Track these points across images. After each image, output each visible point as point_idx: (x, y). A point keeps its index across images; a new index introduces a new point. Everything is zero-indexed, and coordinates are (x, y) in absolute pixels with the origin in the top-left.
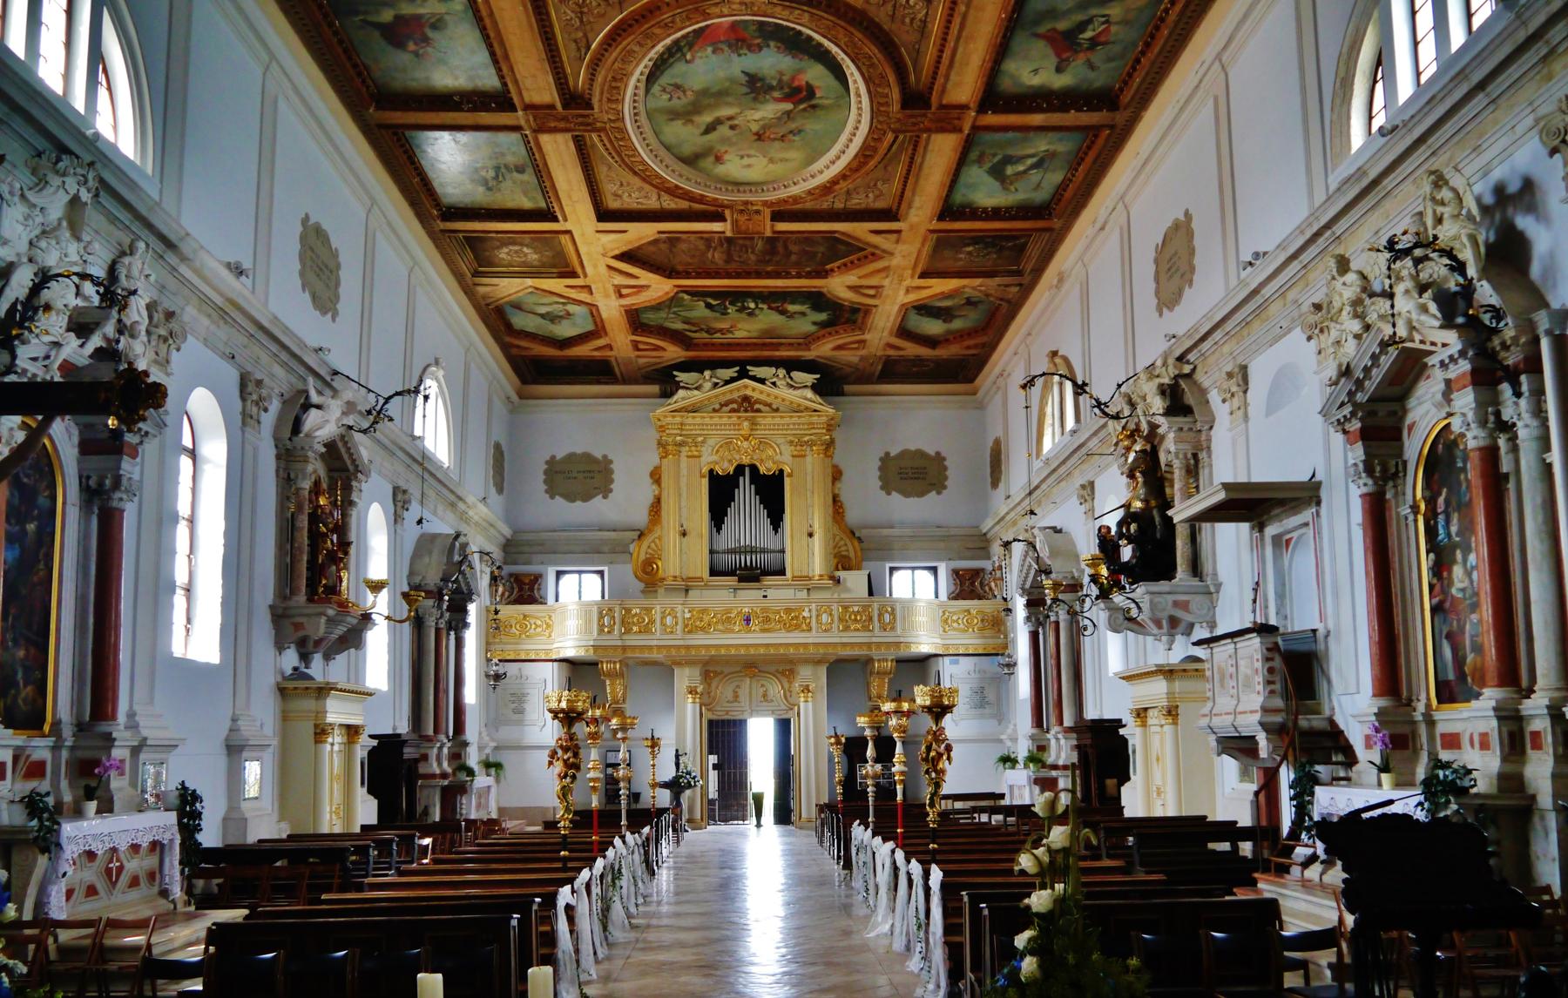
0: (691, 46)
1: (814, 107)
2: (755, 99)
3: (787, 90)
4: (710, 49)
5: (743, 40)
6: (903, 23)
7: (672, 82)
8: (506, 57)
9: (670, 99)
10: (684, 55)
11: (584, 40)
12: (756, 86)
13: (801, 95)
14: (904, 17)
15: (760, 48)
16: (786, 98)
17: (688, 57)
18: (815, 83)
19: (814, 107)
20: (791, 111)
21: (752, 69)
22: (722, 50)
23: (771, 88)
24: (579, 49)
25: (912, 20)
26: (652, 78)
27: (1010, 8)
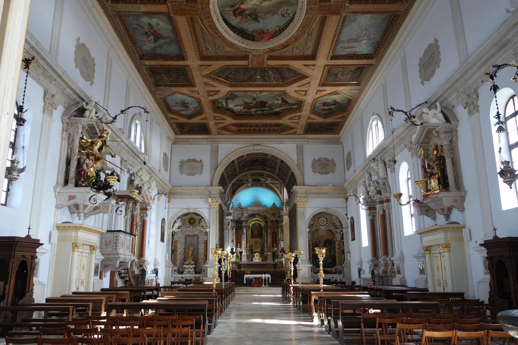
0: (276, 32)
1: (232, 6)
2: (255, 10)
3: (243, 14)
4: (270, 31)
5: (259, 34)
6: (211, 42)
7: (285, 18)
8: (335, 36)
9: (287, 10)
10: (279, 29)
11: (309, 36)
12: (255, 16)
13: (238, 12)
14: (211, 44)
15: (254, 30)
16: (243, 11)
17: (277, 28)
18: (234, 17)
19: (232, 6)
20: (241, 4)
21: (257, 22)
22: (266, 31)
23: (249, 15)
24: (312, 33)
25: (209, 43)
26: (292, 20)
27: (184, 53)
